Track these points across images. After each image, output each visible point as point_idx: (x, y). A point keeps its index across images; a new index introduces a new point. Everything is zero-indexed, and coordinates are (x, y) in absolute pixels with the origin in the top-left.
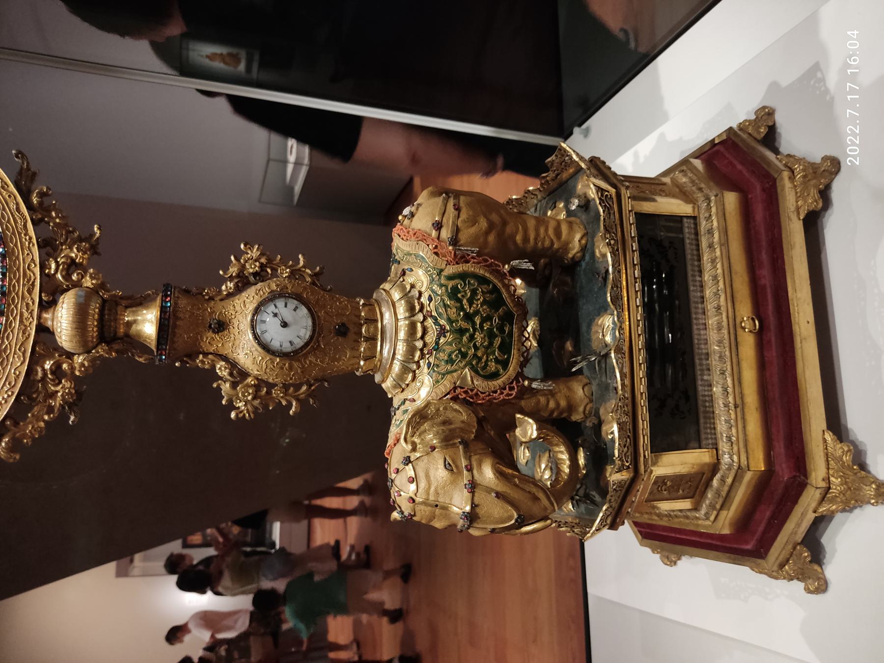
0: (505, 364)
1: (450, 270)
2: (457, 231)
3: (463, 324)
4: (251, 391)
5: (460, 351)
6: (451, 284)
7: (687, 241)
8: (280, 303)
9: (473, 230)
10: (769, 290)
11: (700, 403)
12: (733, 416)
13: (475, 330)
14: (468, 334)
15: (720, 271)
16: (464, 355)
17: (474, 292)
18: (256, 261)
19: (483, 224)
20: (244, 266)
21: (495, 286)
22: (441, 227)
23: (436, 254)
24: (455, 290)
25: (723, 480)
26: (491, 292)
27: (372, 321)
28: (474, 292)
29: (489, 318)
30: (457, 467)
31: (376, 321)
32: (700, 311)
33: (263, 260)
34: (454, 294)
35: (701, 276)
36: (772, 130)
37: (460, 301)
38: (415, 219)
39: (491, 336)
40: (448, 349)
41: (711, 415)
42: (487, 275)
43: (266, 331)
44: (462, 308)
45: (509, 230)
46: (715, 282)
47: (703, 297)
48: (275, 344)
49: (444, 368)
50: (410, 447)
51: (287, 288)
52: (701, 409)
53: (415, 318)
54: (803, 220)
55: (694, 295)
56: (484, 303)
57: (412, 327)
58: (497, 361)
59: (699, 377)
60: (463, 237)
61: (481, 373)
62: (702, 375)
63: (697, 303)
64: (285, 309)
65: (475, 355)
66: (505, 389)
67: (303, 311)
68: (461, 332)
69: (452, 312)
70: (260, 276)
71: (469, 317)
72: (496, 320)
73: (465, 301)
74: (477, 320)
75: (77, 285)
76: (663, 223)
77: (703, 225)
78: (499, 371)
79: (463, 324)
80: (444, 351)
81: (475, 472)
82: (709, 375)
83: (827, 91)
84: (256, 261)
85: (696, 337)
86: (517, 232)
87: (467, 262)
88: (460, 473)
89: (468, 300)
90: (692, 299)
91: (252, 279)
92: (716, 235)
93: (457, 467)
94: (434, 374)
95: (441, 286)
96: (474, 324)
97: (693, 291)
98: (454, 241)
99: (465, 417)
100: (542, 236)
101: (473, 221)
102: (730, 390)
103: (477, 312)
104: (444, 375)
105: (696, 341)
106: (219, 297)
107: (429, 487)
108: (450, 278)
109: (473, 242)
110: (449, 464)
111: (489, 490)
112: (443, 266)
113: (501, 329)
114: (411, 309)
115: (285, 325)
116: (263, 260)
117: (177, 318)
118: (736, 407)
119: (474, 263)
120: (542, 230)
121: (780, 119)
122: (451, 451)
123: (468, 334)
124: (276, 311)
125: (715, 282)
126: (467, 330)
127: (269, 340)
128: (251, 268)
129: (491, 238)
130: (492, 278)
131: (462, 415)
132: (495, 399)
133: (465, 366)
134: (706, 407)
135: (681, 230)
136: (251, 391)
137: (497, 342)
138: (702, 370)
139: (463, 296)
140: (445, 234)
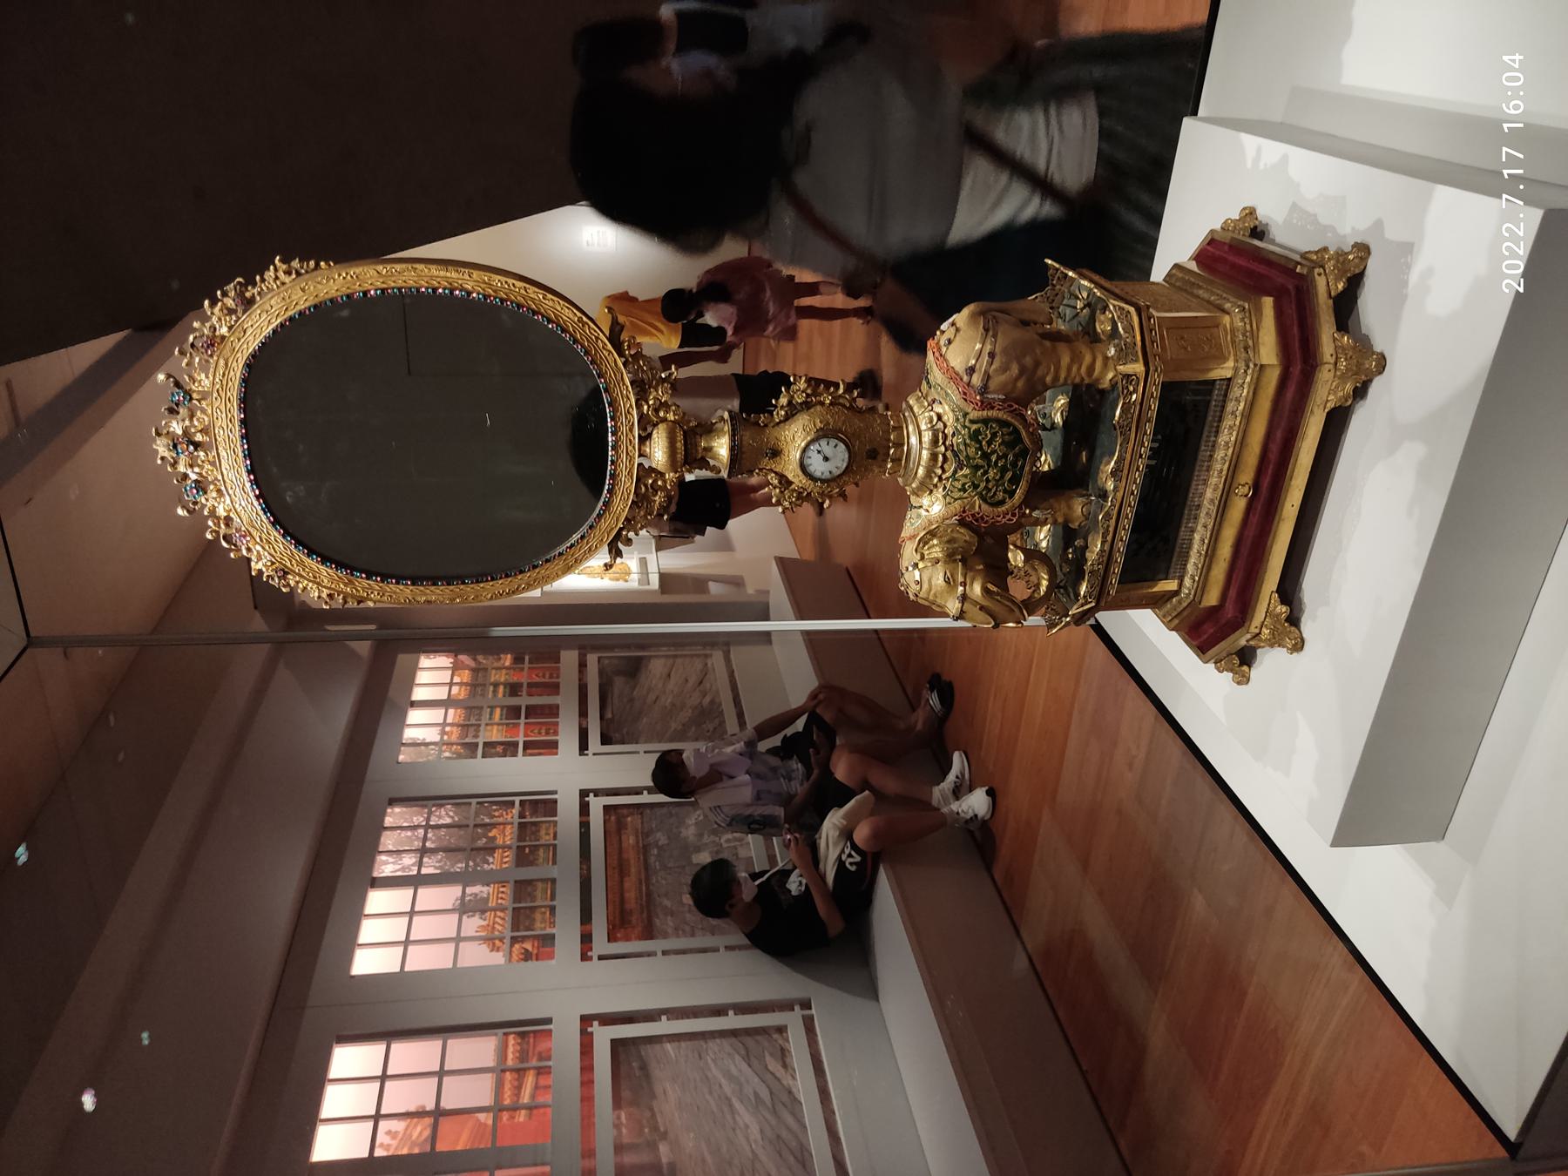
0: (1012, 494)
1: (974, 415)
2: (987, 377)
3: (980, 462)
4: (795, 495)
5: (973, 483)
6: (974, 427)
7: (1214, 403)
8: (823, 442)
9: (1003, 378)
10: (1271, 467)
11: (1178, 545)
12: (1202, 561)
13: (989, 466)
14: (982, 471)
15: (1233, 439)
16: (975, 487)
17: (994, 435)
18: (803, 392)
19: (1015, 369)
20: (793, 397)
21: (1015, 428)
22: (974, 371)
23: (966, 400)
24: (977, 432)
25: (1180, 602)
26: (1009, 434)
27: (899, 445)
28: (994, 435)
29: (1005, 456)
30: (954, 581)
31: (903, 445)
32: (1204, 468)
33: (809, 391)
34: (975, 436)
35: (1216, 436)
36: (1355, 282)
37: (980, 443)
38: (951, 347)
39: (1004, 470)
40: (963, 480)
41: (1185, 556)
42: (1009, 419)
43: (811, 465)
44: (981, 448)
45: (1040, 373)
46: (1226, 448)
47: (1211, 456)
48: (818, 474)
49: (957, 495)
50: (918, 557)
51: (829, 424)
52: (1177, 550)
53: (938, 449)
54: (1328, 413)
55: (1203, 453)
56: (1003, 443)
57: (934, 457)
58: (1005, 491)
59: (1184, 525)
60: (993, 385)
61: (989, 501)
62: (1187, 523)
63: (1204, 461)
64: (826, 446)
65: (986, 487)
66: (1008, 514)
67: (842, 446)
68: (977, 468)
69: (971, 451)
70: (807, 406)
71: (986, 456)
72: (1010, 457)
73: (984, 443)
74: (994, 458)
75: (664, 420)
76: (1193, 387)
77: (1235, 392)
78: (1005, 499)
79: (980, 462)
80: (959, 480)
81: (967, 587)
82: (1194, 523)
83: (1405, 283)
84: (803, 392)
85: (1192, 491)
86: (1047, 374)
87: (993, 408)
88: (956, 587)
89: (987, 442)
90: (1200, 457)
91: (799, 408)
92: (1242, 404)
93: (954, 581)
94: (948, 497)
95: (964, 427)
96: (990, 460)
97: (1204, 450)
98: (984, 389)
99: (967, 538)
100: (1073, 375)
101: (1004, 368)
102: (1206, 541)
103: (994, 452)
104: (956, 500)
105: (1191, 495)
106: (772, 424)
107: (930, 590)
108: (972, 422)
109: (1002, 389)
110: (948, 578)
111: (975, 603)
112: (970, 410)
113: (1014, 464)
114: (935, 442)
115: (826, 459)
116: (809, 391)
117: (743, 453)
118: (1206, 557)
119: (998, 409)
120: (1075, 369)
121: (1373, 268)
122: (952, 565)
123: (982, 471)
124: (820, 449)
125: (1226, 448)
126: (982, 467)
127: (813, 471)
128: (799, 399)
129: (1020, 384)
130: (1013, 421)
131: (964, 535)
132: (998, 522)
133: (975, 495)
134: (1183, 548)
135: (1210, 392)
136: (795, 495)
137: (1009, 475)
138: (1189, 519)
139: (983, 438)
140: (976, 380)
